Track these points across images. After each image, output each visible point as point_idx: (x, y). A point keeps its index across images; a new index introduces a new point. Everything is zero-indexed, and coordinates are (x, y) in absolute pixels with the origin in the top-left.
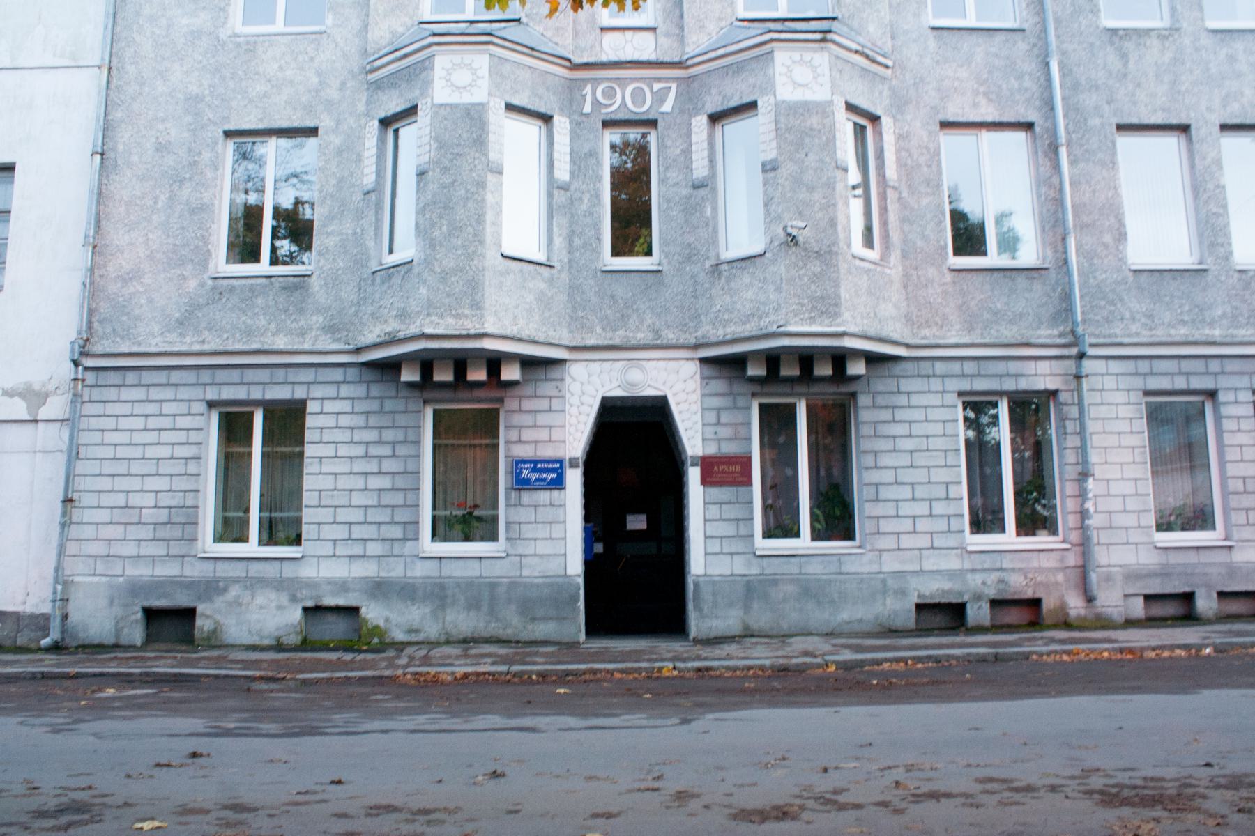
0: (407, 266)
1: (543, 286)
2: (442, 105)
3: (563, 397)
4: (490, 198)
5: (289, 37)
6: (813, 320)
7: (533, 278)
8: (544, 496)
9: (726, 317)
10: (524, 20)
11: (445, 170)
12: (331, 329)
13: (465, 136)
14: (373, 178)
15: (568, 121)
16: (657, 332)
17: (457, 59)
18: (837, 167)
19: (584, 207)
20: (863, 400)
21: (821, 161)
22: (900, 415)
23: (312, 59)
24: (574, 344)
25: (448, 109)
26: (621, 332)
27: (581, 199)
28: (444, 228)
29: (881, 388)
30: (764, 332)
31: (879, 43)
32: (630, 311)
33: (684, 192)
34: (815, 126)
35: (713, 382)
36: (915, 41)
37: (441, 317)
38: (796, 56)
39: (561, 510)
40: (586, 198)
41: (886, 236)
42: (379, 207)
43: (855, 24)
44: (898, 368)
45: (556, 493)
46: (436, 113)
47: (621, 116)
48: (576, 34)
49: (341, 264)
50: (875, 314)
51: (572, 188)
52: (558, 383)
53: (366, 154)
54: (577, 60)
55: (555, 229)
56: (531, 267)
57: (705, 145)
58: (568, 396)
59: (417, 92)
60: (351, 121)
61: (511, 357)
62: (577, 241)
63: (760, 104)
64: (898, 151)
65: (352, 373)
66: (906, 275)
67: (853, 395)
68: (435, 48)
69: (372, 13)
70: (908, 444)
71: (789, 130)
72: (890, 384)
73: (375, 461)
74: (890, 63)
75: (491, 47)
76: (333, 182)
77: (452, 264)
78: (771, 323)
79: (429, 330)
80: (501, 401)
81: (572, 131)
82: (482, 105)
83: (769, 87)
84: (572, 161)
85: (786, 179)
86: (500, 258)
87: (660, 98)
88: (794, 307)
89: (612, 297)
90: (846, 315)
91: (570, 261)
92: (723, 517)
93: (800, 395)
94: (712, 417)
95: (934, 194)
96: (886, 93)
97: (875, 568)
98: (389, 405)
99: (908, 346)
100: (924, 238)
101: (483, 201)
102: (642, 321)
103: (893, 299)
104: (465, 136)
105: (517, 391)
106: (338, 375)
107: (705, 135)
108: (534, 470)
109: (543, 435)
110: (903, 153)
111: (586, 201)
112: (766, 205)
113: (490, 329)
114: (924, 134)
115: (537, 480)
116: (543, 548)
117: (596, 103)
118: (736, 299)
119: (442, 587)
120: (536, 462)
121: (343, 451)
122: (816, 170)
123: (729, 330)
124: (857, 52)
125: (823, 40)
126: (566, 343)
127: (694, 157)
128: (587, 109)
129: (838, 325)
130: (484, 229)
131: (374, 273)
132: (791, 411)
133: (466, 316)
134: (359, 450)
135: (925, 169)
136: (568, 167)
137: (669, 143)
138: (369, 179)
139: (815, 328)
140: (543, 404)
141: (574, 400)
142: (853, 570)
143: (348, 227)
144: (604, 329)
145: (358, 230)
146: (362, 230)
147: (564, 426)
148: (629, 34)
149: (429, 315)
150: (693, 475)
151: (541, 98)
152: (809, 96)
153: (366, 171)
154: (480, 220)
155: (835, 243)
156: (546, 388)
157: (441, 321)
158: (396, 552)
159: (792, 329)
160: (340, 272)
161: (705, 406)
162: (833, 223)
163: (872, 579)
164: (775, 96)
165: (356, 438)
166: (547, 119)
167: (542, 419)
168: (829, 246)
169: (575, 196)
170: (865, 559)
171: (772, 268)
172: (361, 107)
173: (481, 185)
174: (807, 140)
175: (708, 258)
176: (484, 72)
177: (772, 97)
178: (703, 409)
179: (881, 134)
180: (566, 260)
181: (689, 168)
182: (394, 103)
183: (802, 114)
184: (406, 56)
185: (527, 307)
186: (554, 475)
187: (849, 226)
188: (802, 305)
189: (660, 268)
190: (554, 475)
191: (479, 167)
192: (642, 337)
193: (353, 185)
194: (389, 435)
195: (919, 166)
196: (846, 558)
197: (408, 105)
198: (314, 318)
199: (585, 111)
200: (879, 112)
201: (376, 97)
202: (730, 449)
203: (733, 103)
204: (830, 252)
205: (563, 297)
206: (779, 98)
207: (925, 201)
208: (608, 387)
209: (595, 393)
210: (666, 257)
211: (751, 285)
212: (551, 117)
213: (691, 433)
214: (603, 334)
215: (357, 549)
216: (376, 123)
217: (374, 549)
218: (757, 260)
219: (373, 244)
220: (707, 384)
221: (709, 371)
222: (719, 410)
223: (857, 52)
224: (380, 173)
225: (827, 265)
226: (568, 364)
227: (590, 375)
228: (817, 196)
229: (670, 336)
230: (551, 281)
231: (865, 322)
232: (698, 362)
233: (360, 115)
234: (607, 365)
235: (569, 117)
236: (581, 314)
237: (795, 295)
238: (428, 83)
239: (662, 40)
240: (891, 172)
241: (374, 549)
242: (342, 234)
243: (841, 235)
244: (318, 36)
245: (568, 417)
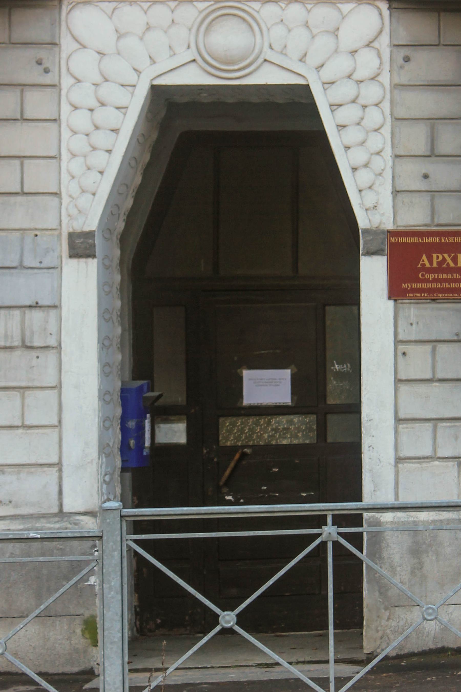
52: (42, 54)
58: (66, 82)
92: (440, 375)
147: (57, 158)
161: (401, 113)
178: (397, 119)
209: (132, 78)
220: (407, 59)
227: (120, 36)
245: (65, 134)
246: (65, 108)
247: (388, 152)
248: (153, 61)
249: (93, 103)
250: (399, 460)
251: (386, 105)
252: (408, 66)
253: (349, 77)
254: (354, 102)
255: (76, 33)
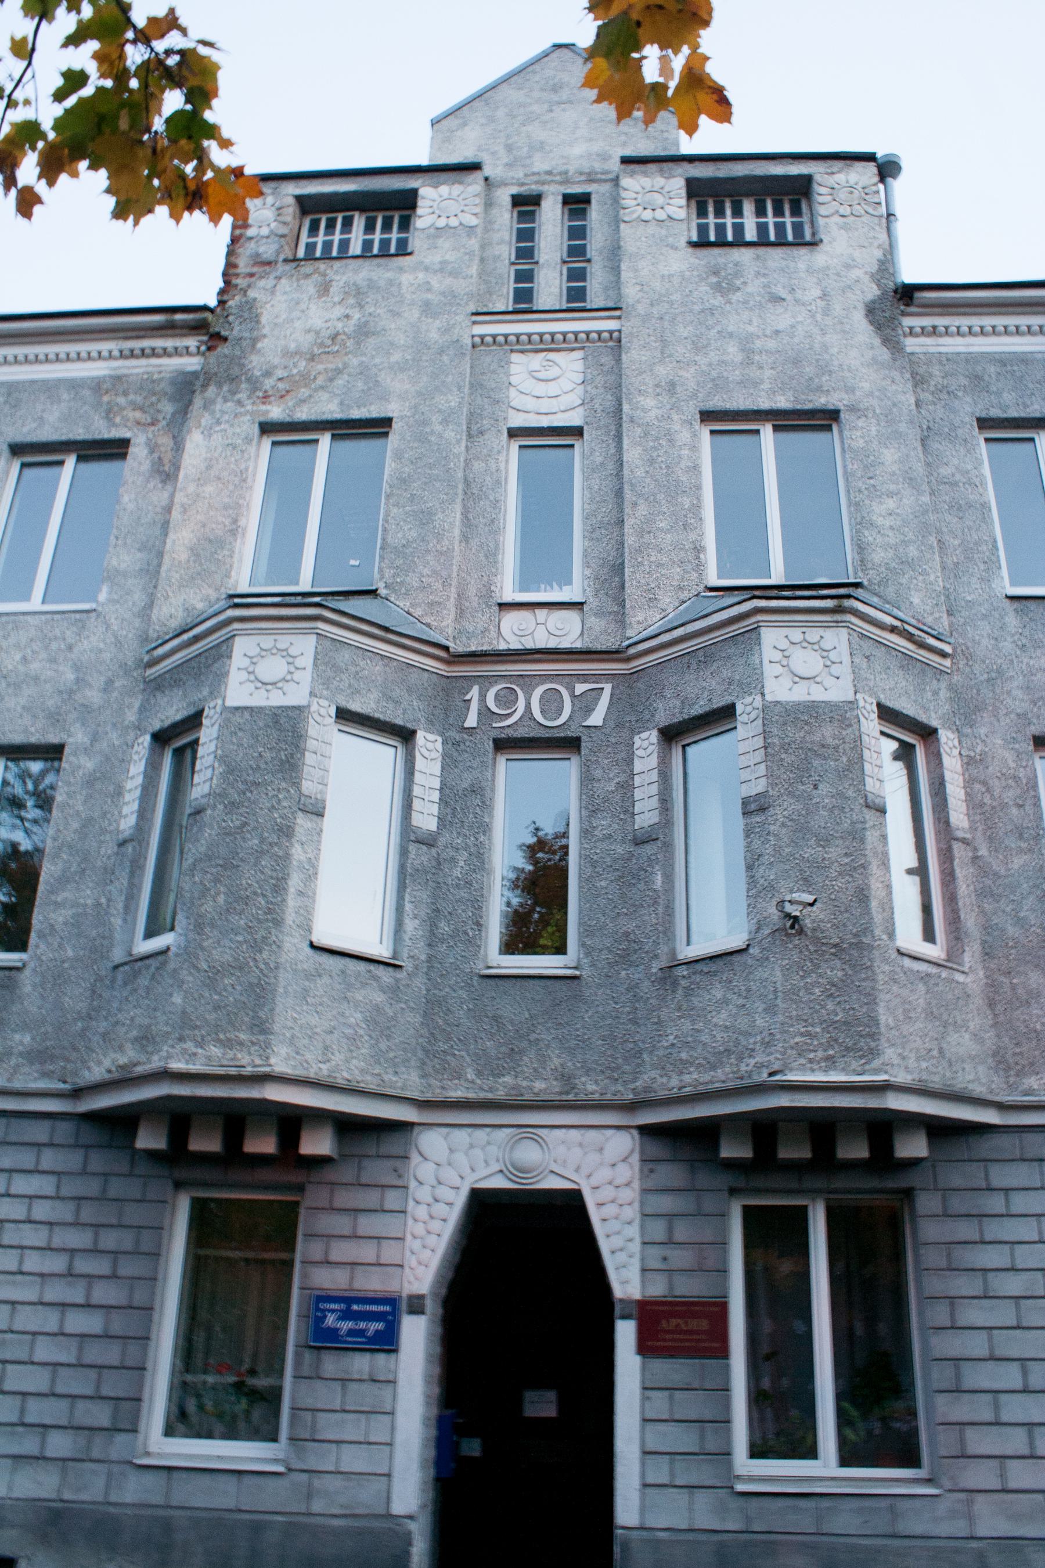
0: (160, 958)
1: (379, 998)
2: (237, 709)
3: (406, 1187)
4: (297, 853)
5: (43, 617)
6: (831, 1062)
7: (364, 985)
8: (361, 1363)
9: (684, 1055)
10: (383, 592)
11: (232, 806)
12: (38, 1056)
13: (268, 755)
14: (132, 820)
15: (440, 739)
16: (567, 1079)
17: (267, 642)
18: (868, 806)
19: (457, 872)
20: (927, 1203)
21: (841, 795)
22: (994, 1230)
23: (70, 648)
24: (428, 1096)
25: (247, 715)
26: (508, 1079)
27: (453, 860)
28: (221, 899)
29: (958, 1182)
30: (746, 1082)
31: (929, 620)
32: (524, 1044)
33: (620, 850)
34: (830, 741)
35: (663, 1169)
36: (985, 617)
37: (200, 1044)
38: (796, 635)
39: (387, 1392)
40: (462, 858)
41: (954, 920)
42: (136, 867)
43: (890, 592)
44: (986, 1146)
45: (381, 1358)
46: (228, 720)
47: (522, 732)
48: (461, 613)
49: (70, 953)
50: (941, 1051)
51: (442, 841)
52: (398, 1163)
53: (129, 785)
54: (457, 647)
55: (408, 907)
56: (362, 966)
57: (654, 776)
58: (413, 1184)
59: (206, 691)
60: (114, 737)
61: (319, 1116)
62: (444, 927)
63: (739, 708)
64: (969, 783)
65: (64, 1131)
66: (992, 986)
67: (908, 1194)
68: (236, 625)
69: (162, 583)
70: (1014, 1285)
71: (785, 747)
72: (973, 1173)
73: (82, 1284)
74: (948, 649)
75: (321, 625)
76: (75, 825)
77: (227, 958)
78: (759, 1066)
79: (177, 1065)
80: (301, 1188)
81: (445, 755)
82: (299, 709)
83: (755, 683)
84: (443, 801)
85: (783, 825)
86: (308, 950)
87: (585, 704)
88: (797, 1040)
89: (496, 1018)
90: (890, 1054)
91: (430, 959)
92: (677, 1417)
93: (814, 1193)
94: (658, 1230)
95: (1031, 851)
96: (944, 694)
97: (959, 1527)
98: (117, 1188)
99: (1001, 1107)
100: (1020, 921)
101: (287, 856)
102: (543, 1059)
103: (971, 1025)
104: (268, 755)
105: (330, 1174)
106: (39, 1132)
107: (654, 761)
108: (347, 1315)
109: (367, 1252)
110: (977, 786)
111: (462, 863)
112: (749, 867)
113: (279, 1065)
114: (1009, 756)
115: (351, 1332)
116: (353, 1460)
117: (485, 713)
118: (699, 1025)
119: (167, 1526)
120: (349, 1300)
121: (33, 1262)
122: (831, 810)
123: (687, 1078)
124: (893, 629)
125: (838, 610)
126: (415, 1095)
127: (638, 794)
128: (471, 721)
129: (876, 1071)
130: (284, 900)
131: (116, 967)
132: (799, 1219)
133: (241, 1044)
134: (57, 1264)
135: (1014, 811)
136: (435, 809)
137: (598, 773)
138: (128, 822)
139: (836, 1077)
140: (368, 1199)
141: (424, 1194)
142: (919, 1529)
143: (88, 895)
144: (479, 1074)
145: (103, 900)
146: (109, 900)
147: (402, 1239)
148: (541, 614)
149: (181, 1039)
150: (626, 1333)
151: (397, 703)
152: (818, 694)
153: (126, 810)
154: (279, 887)
155: (867, 930)
156: (376, 1171)
157: (200, 1051)
158: (96, 1454)
159: (793, 1077)
160: (66, 965)
161: (649, 1210)
162: (862, 896)
163: (957, 1551)
164: (763, 694)
165: (56, 1242)
166: (405, 736)
167: (367, 1225)
168: (856, 935)
169: (444, 855)
170: (942, 1507)
171: (761, 973)
172: (131, 717)
173: (286, 832)
174: (816, 763)
175: (656, 956)
176: (307, 661)
177: (759, 698)
178: (644, 1215)
179: (938, 756)
180: (423, 957)
181: (628, 810)
182: (175, 708)
183: (807, 723)
184: (197, 639)
185: (349, 1031)
186: (380, 1326)
187: (891, 900)
188: (808, 1034)
189: (577, 973)
190: (380, 1326)
191: (285, 804)
192: (541, 1087)
193: (103, 831)
194: (110, 1240)
195: (1004, 806)
196: (907, 1504)
197: (192, 711)
198: (17, 1037)
199: (466, 725)
200: (934, 723)
201: (153, 701)
202: (689, 1288)
203: (699, 709)
204: (859, 946)
205: (416, 1019)
206: (769, 698)
207: (1017, 862)
208: (483, 1172)
209: (457, 1182)
210: (588, 954)
211: (726, 1001)
212: (413, 732)
213: (622, 1257)
214: (478, 1081)
215: (29, 1445)
216: (148, 738)
217: (59, 1444)
218: (736, 958)
219: (120, 922)
220: (652, 1171)
221: (656, 1149)
222: (670, 1217)
223: (893, 629)
224: (144, 814)
225: (853, 967)
226: (416, 1130)
228: (834, 852)
229: (590, 1087)
230: (394, 991)
231: (924, 1065)
232: (635, 1132)
233: (128, 727)
234: (481, 1134)
235: (442, 734)
236: (442, 1046)
237: (799, 1018)
238: (222, 676)
239: (592, 621)
240: (959, 816)
241: (59, 1444)
242: (78, 905)
243: (878, 917)
244: (85, 615)
245: (410, 1222)
246: (411, 1203)
247: (638, 1240)
248: (473, 1170)
249: (430, 1200)
250: (645, 1485)
251: (636, 1205)
252: (653, 1176)
253: (610, 1183)
254: (613, 1202)
255: (421, 1150)
